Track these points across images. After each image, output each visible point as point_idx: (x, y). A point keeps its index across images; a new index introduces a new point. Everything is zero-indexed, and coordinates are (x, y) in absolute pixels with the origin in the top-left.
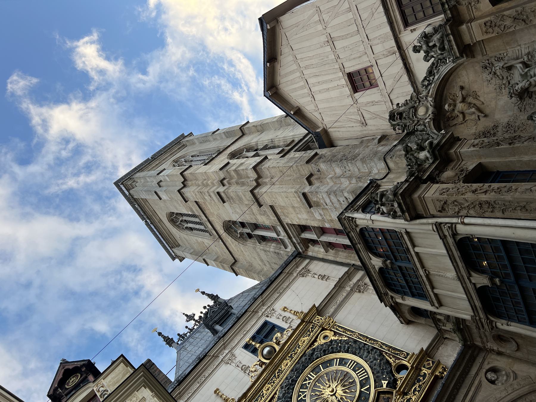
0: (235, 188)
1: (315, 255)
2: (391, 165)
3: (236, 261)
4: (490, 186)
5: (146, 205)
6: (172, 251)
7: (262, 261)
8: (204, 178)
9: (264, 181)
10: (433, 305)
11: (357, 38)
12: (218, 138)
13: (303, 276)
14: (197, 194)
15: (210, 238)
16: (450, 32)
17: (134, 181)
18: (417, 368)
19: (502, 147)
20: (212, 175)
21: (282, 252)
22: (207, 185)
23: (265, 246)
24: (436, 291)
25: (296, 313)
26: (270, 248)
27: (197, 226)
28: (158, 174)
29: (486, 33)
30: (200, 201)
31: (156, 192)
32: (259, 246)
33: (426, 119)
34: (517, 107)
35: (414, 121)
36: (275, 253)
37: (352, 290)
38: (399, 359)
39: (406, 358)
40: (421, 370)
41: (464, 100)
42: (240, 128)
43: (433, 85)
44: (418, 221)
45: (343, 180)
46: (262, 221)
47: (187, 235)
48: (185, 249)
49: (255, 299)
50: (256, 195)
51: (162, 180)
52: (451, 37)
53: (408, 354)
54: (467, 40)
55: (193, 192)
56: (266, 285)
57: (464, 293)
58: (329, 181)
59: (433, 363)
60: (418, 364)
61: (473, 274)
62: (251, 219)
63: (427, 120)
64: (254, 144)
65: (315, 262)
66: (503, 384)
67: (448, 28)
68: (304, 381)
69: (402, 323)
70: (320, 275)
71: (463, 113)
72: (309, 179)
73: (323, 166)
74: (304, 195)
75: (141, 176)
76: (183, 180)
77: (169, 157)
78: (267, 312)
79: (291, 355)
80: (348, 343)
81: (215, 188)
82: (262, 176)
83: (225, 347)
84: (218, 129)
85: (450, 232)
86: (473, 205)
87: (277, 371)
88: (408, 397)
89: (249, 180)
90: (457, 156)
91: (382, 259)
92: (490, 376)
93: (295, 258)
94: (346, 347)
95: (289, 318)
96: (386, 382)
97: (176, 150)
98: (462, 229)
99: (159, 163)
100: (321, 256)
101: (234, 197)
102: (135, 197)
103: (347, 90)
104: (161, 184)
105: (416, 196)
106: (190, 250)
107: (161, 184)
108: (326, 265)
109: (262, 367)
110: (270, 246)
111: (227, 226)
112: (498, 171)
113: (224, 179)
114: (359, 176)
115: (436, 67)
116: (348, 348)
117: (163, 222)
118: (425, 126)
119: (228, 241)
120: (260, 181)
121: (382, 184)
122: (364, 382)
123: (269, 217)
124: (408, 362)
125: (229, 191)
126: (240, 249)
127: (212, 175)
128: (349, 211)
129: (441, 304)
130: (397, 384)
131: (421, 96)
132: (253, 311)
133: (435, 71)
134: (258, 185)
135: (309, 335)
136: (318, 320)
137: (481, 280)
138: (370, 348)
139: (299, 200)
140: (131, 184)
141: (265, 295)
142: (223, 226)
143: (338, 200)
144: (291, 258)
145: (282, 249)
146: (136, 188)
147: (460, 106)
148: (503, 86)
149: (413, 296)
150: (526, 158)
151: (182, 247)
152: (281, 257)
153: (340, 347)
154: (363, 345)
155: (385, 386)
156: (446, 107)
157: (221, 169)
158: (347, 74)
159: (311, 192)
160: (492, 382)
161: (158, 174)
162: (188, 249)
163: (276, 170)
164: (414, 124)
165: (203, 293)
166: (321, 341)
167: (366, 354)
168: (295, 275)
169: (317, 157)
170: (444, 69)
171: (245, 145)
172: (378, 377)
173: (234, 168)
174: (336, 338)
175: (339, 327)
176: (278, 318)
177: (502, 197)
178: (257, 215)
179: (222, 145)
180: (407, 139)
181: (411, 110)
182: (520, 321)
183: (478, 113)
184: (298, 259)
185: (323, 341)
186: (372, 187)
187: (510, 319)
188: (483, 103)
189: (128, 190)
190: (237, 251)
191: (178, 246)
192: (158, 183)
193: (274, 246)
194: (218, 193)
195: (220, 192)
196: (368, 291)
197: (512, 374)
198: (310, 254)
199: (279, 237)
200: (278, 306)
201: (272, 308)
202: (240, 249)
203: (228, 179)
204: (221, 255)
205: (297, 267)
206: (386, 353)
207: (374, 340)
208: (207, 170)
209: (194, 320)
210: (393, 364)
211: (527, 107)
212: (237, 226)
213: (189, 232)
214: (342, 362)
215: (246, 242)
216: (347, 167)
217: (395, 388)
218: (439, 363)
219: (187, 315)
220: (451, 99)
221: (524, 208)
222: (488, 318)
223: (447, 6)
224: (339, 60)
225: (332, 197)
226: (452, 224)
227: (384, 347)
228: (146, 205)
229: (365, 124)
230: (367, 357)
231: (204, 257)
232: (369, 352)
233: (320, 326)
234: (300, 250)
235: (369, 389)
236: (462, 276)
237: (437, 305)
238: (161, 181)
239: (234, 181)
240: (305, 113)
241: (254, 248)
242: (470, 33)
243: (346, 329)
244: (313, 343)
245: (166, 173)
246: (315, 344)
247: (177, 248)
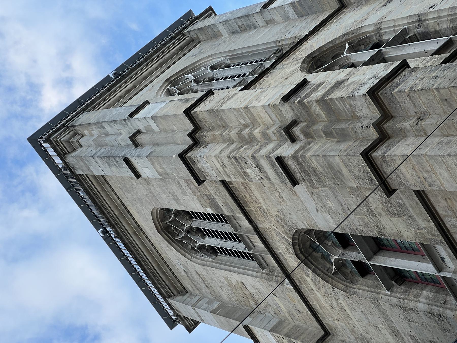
0: (322, 147)
3: (327, 333)
5: (104, 190)
6: (169, 305)
8: (243, 122)
9: (398, 126)
12: (278, 18)
14: (226, 161)
15: (259, 274)
17: (76, 134)
20: (263, 114)
22: (251, 140)
23: (402, 296)
26: (419, 301)
27: (228, 245)
28: (132, 115)
30: (233, 180)
31: (127, 161)
32: (387, 295)
36: (432, 314)
46: (395, 231)
47: (203, 265)
48: (199, 301)
50: (378, 163)
51: (142, 128)
55: (217, 157)
62: (366, 225)
64: (371, 29)
75: (89, 122)
76: (191, 127)
81: (271, 146)
82: (393, 114)
89: (359, 125)
97: (174, 54)
99: (134, 87)
101: (321, 170)
102: (79, 172)
104: (140, 138)
106: (210, 302)
107: (140, 138)
110: (418, 296)
111: (304, 244)
113: (294, 123)
117: (144, 234)
119: (305, 282)
120: (388, 126)
123: (414, 220)
125: (309, 154)
126: (337, 302)
127: (263, 114)
140: (68, 141)
142: (294, 245)
145: (449, 306)
146: (80, 150)
151: (191, 294)
152: (448, 326)
157: (286, 98)
161: (132, 115)
162: (206, 300)
163: (431, 97)
171: (348, 34)
173: (318, 94)
178: (380, 215)
179: (289, 37)
189: (62, 156)
190: (329, 308)
191: (183, 291)
192: (132, 138)
193: (427, 298)
194: (280, 160)
195: (284, 157)
199: (443, 274)
202: (337, 302)
203: (303, 124)
204: (289, 318)
208: (252, 102)
212: (330, 243)
213: (208, 259)
215: (352, 286)
228: (104, 190)
238: (138, 132)
239: (319, 127)
241: (375, 302)
245: (149, 113)
247: (179, 298)
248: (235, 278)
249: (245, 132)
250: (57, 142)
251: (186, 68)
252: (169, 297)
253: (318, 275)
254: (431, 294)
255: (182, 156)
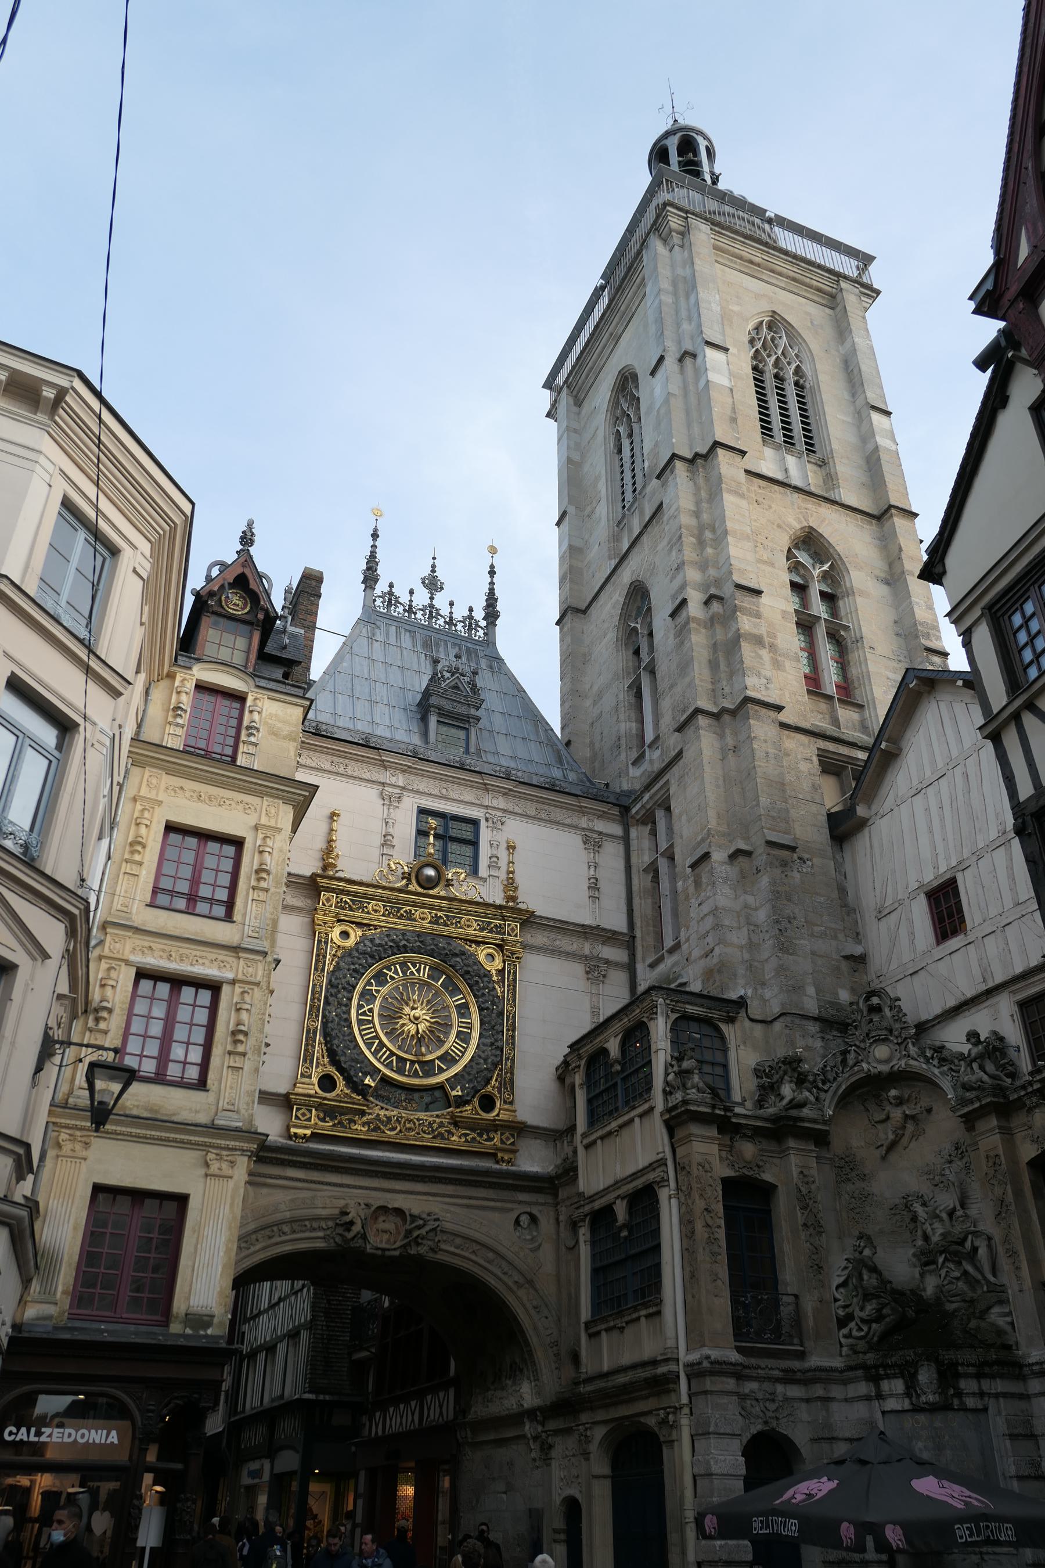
1: (634, 844)
2: (778, 1026)
3: (584, 612)
4: (719, 1227)
7: (600, 695)
10: (584, 1135)
11: (1009, 903)
13: (585, 843)
16: (983, 1102)
18: (495, 1126)
19: (799, 1214)
21: (623, 756)
24: (599, 1142)
25: (511, 884)
28: (708, 343)
29: (987, 1157)
31: (662, 359)
33: (869, 1063)
34: (897, 1201)
35: (863, 1041)
36: (619, 739)
37: (586, 957)
38: (500, 1092)
39: (505, 1102)
40: (496, 1131)
41: (906, 1117)
42: (891, 507)
43: (924, 1066)
44: (664, 1131)
45: (745, 930)
49: (507, 777)
52: (977, 1105)
53: (511, 1103)
54: (982, 1126)
56: (542, 779)
57: (606, 1185)
58: (742, 898)
59: (513, 1144)
60: (501, 1126)
61: (625, 1202)
63: (865, 1066)
65: (621, 848)
66: (519, 1237)
67: (988, 1100)
68: (412, 964)
69: (557, 1069)
70: (597, 879)
71: (888, 1118)
72: (736, 855)
73: (765, 881)
74: (706, 856)
77: (783, 282)
78: (494, 813)
79: (441, 917)
80: (493, 1004)
83: (406, 770)
84: (888, 414)
85: (658, 1179)
86: (690, 1212)
87: (408, 908)
88: (454, 1131)
89: (725, 683)
90: (784, 1151)
91: (620, 1057)
92: (525, 1220)
93: (615, 805)
94: (487, 1005)
95: (499, 868)
96: (460, 1093)
97: (810, 287)
98: (663, 1194)
99: (759, 265)
100: (634, 860)
103: (930, 877)
105: (695, 1129)
107: (688, 361)
108: (621, 877)
109: (403, 879)
112: (770, 1211)
113: (720, 599)
114: (756, 964)
115: (951, 1069)
116: (487, 1009)
118: (855, 1065)
120: (726, 718)
121: (737, 1024)
122: (448, 1059)
124: (500, 1109)
128: (668, 1002)
129: (587, 1147)
130: (464, 1105)
131: (910, 1045)
132: (485, 784)
133: (945, 1068)
134: (716, 716)
135: (482, 929)
136: (513, 930)
137: (621, 1210)
138: (499, 1044)
139: (699, 838)
140: (671, 231)
141: (522, 789)
143: (708, 932)
144: (612, 799)
147: (897, 1114)
148: (931, 1177)
149: (590, 1101)
150: (787, 1247)
151: (579, 414)
153: (483, 995)
154: (500, 1029)
155: (454, 1093)
156: (893, 1093)
157: (739, 587)
158: (955, 877)
159: (711, 871)
160: (517, 1222)
161: (708, 343)
164: (858, 1043)
165: (492, 573)
166: (482, 954)
167: (488, 1041)
168: (583, 822)
169: (785, 853)
170: (946, 1084)
171: (841, 559)
172: (463, 1076)
174: (495, 978)
175: (515, 973)
176: (491, 845)
177: (701, 1250)
180: (835, 1033)
181: (884, 1032)
182: (594, 1256)
183: (886, 1143)
184: (615, 811)
185: (482, 957)
186: (728, 1012)
187: (593, 1243)
188: (905, 1148)
189: (656, 227)
191: (579, 403)
192: (686, 354)
193: (631, 730)
194: (684, 601)
196: (594, 987)
197: (537, 1244)
198: (633, 833)
200: (516, 829)
201: (504, 819)
205: (599, 817)
206: (501, 1070)
207: (513, 1043)
209: (432, 598)
210: (489, 1088)
211: (898, 1217)
214: (463, 1009)
216: (767, 937)
217: (458, 1107)
218: (515, 1152)
219: (433, 571)
220: (910, 1096)
221: (693, 1276)
222: (586, 1216)
223: (1022, 1093)
224: (975, 858)
225: (709, 922)
226: (668, 1180)
227: (509, 1063)
229: (881, 915)
230: (484, 1045)
231: (571, 510)
232: (492, 1044)
233: (503, 940)
234: (634, 811)
235: (441, 1070)
236: (619, 1188)
237: (585, 1142)
240: (890, 769)
242: (987, 1131)
243: (515, 986)
244: (472, 941)
246: (474, 946)
247: (571, 401)
248: (602, 487)
249: (708, 534)
250: (666, 216)
251: (793, 327)
252: (568, 387)
253: (622, 609)
254: (634, 732)
255: (674, 456)
